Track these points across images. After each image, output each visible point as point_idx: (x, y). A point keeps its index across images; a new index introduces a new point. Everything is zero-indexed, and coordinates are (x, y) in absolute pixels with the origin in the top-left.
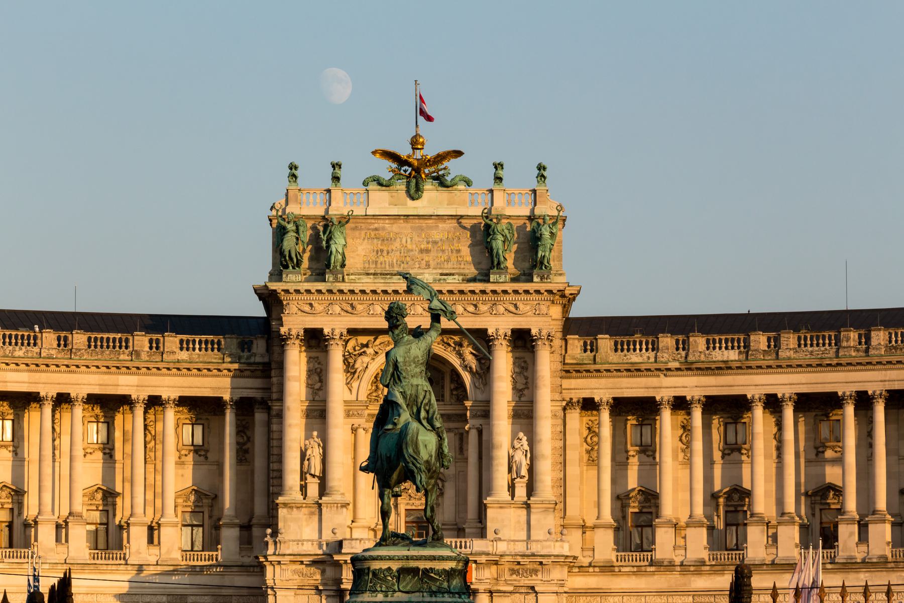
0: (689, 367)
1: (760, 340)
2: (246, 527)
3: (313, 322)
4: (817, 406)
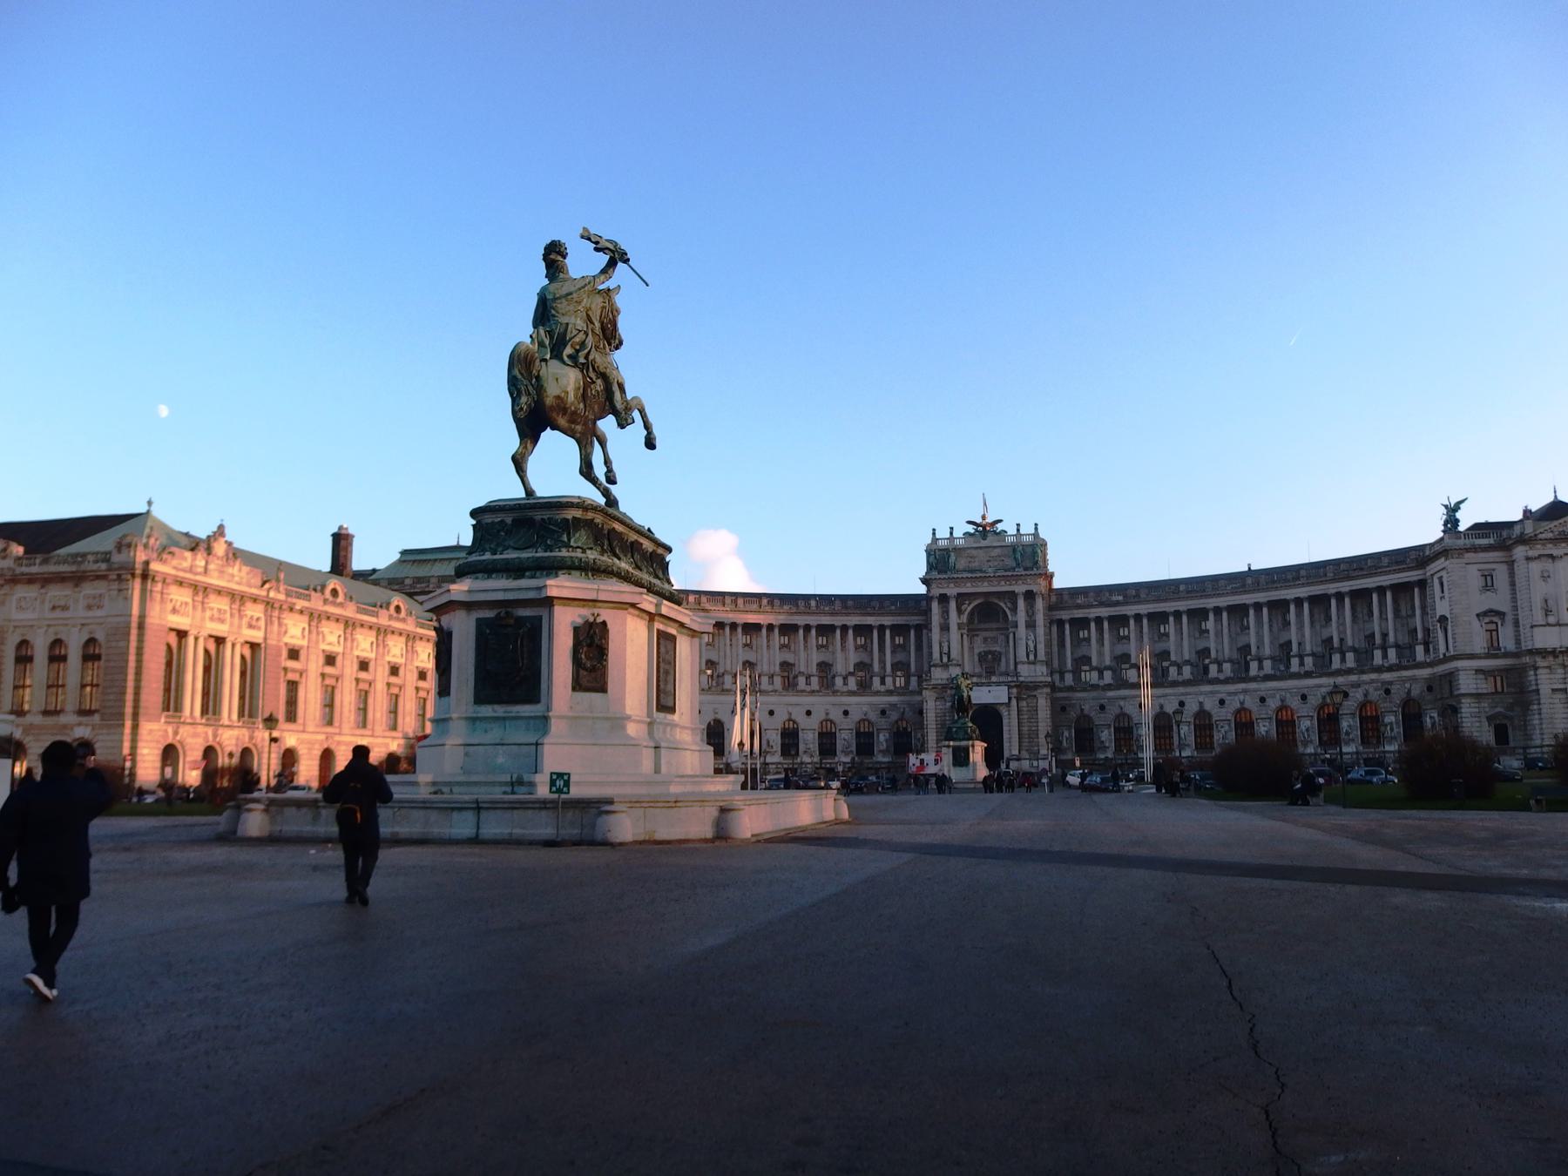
2: (920, 677)
3: (942, 591)
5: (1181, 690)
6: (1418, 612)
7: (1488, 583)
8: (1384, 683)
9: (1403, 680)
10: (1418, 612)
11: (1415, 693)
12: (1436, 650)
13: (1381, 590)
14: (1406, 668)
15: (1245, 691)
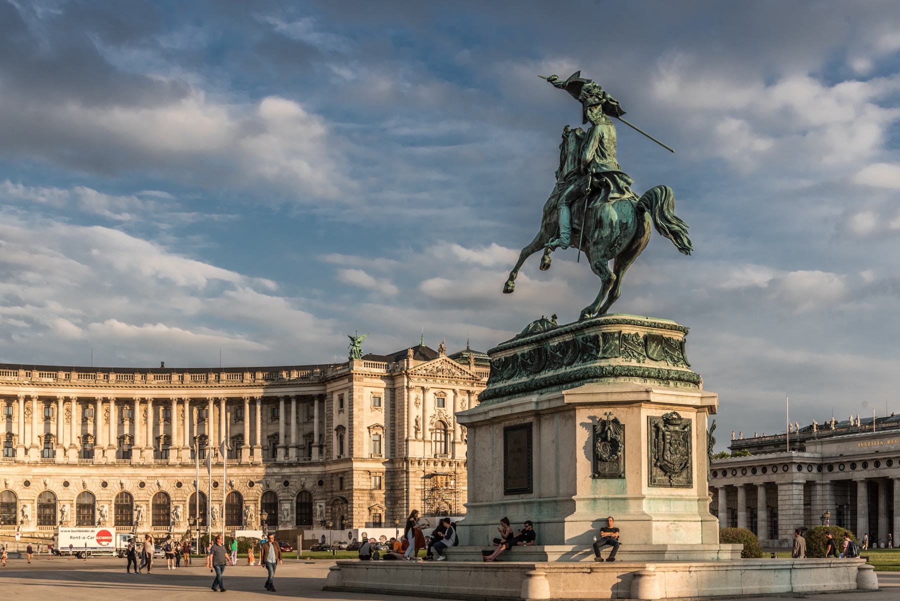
0: (33, 384)
1: (62, 375)
4: (86, 402)
5: (105, 471)
6: (316, 420)
7: (377, 401)
8: (283, 476)
9: (300, 475)
10: (316, 420)
11: (308, 486)
12: (329, 452)
13: (288, 400)
14: (303, 465)
15: (164, 476)
